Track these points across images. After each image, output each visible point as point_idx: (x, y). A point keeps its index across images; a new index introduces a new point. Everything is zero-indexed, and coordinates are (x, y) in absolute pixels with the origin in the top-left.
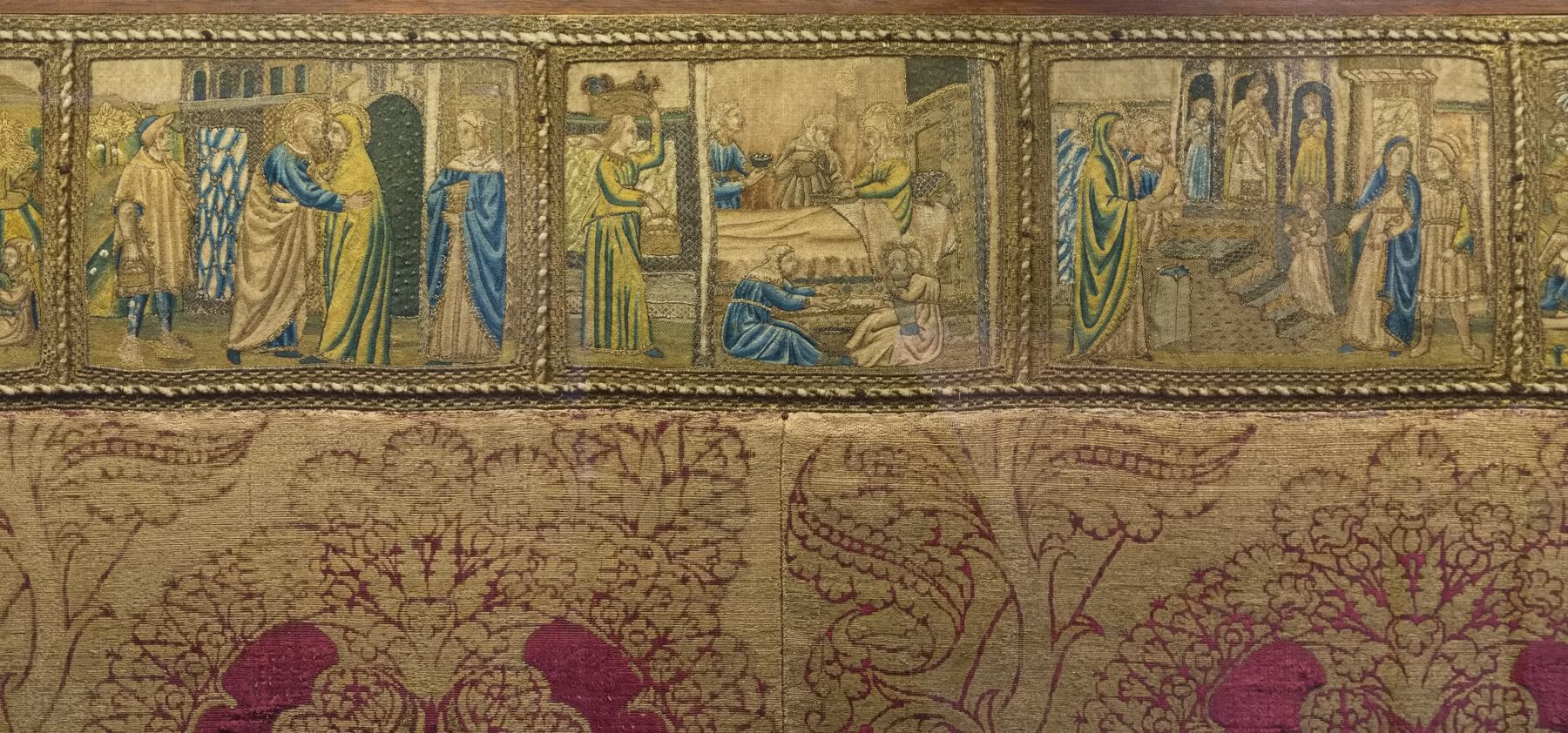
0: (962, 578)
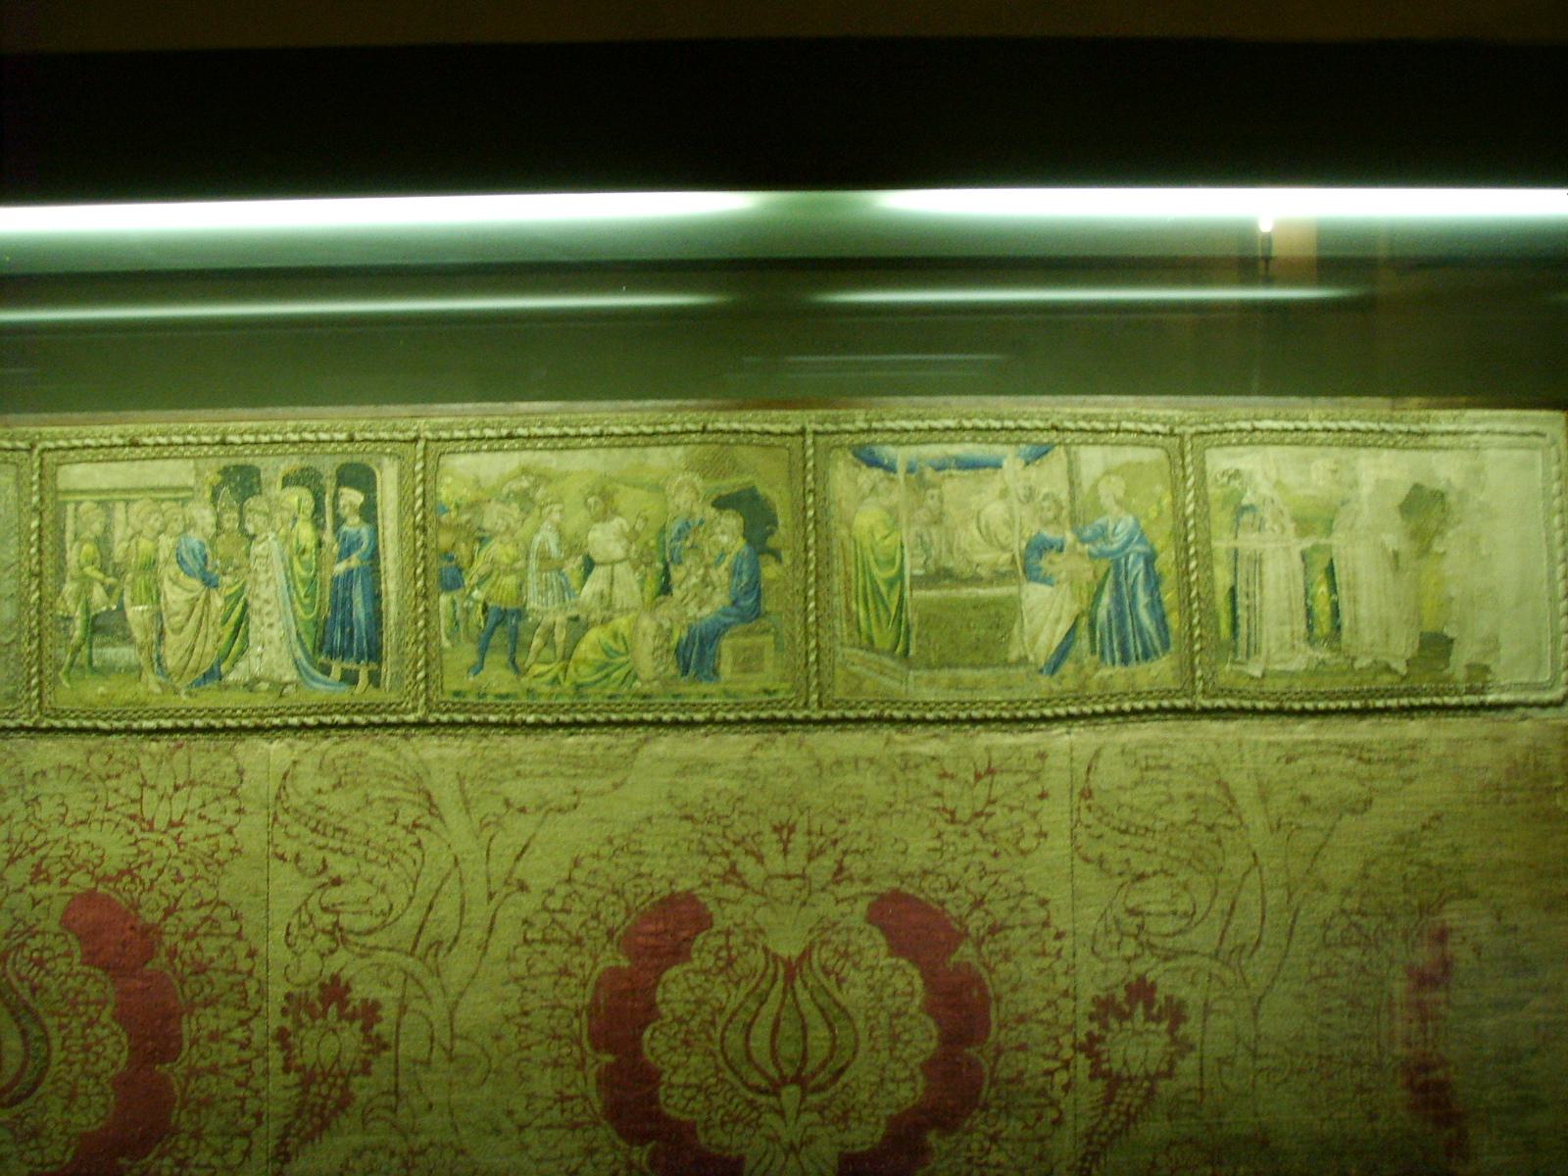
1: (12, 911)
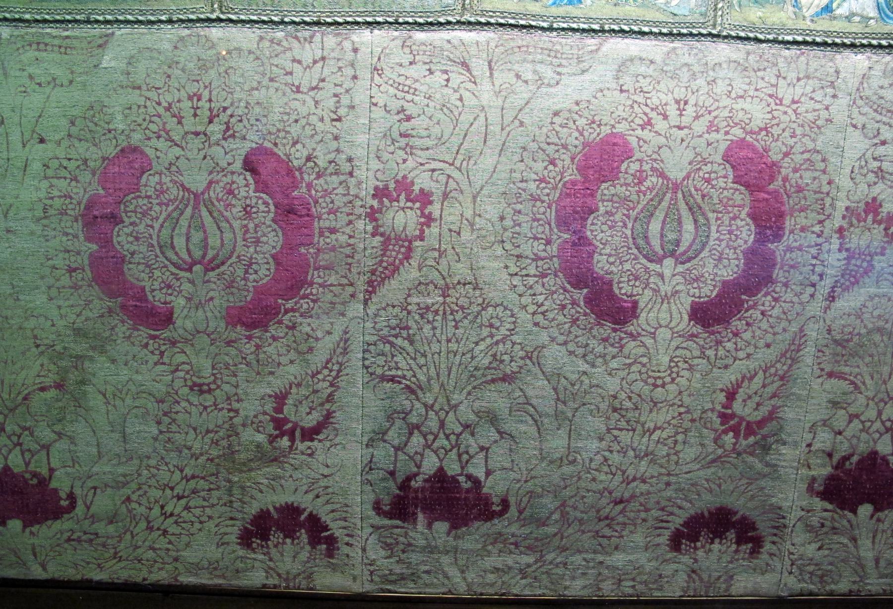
0: (459, 103)
1: (695, 148)
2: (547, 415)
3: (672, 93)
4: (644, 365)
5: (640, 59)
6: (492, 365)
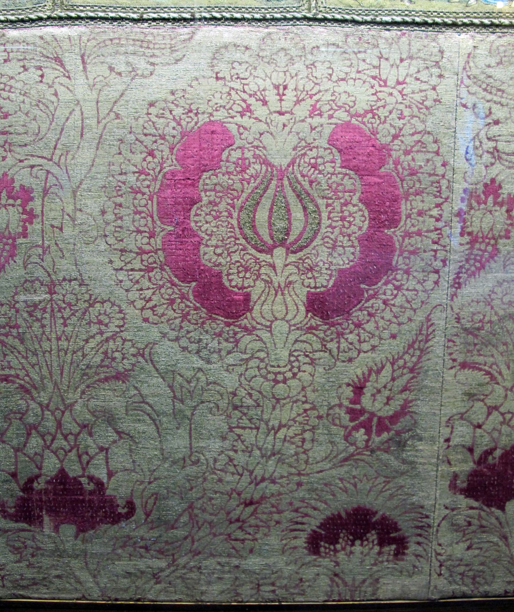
0: (54, 99)
1: (298, 134)
2: (165, 414)
3: (270, 78)
4: (262, 360)
5: (235, 45)
6: (104, 363)
